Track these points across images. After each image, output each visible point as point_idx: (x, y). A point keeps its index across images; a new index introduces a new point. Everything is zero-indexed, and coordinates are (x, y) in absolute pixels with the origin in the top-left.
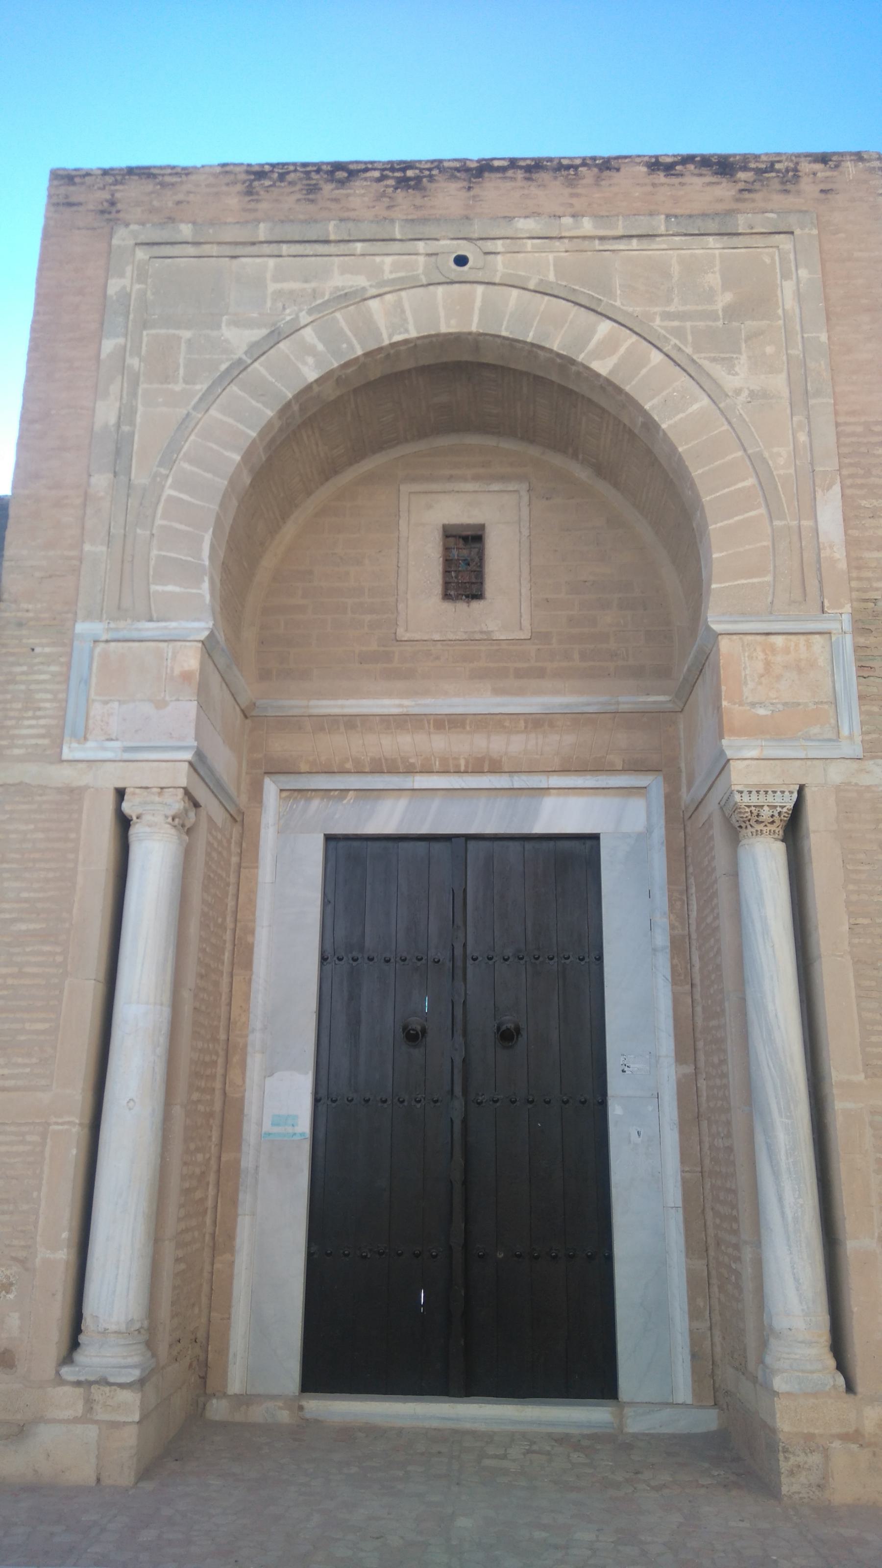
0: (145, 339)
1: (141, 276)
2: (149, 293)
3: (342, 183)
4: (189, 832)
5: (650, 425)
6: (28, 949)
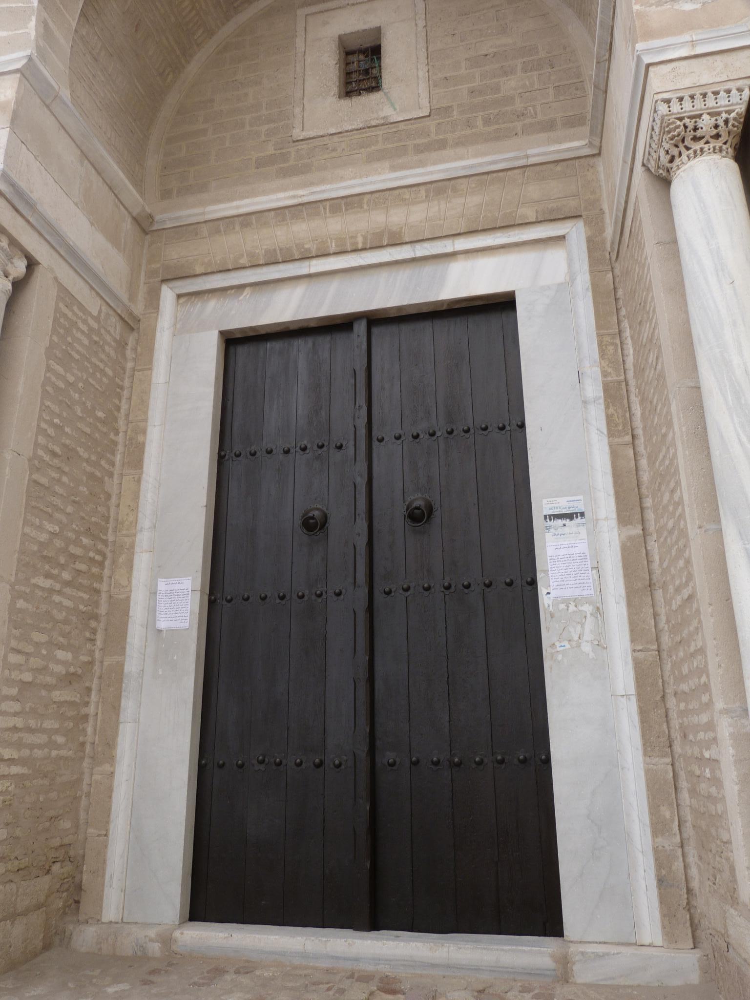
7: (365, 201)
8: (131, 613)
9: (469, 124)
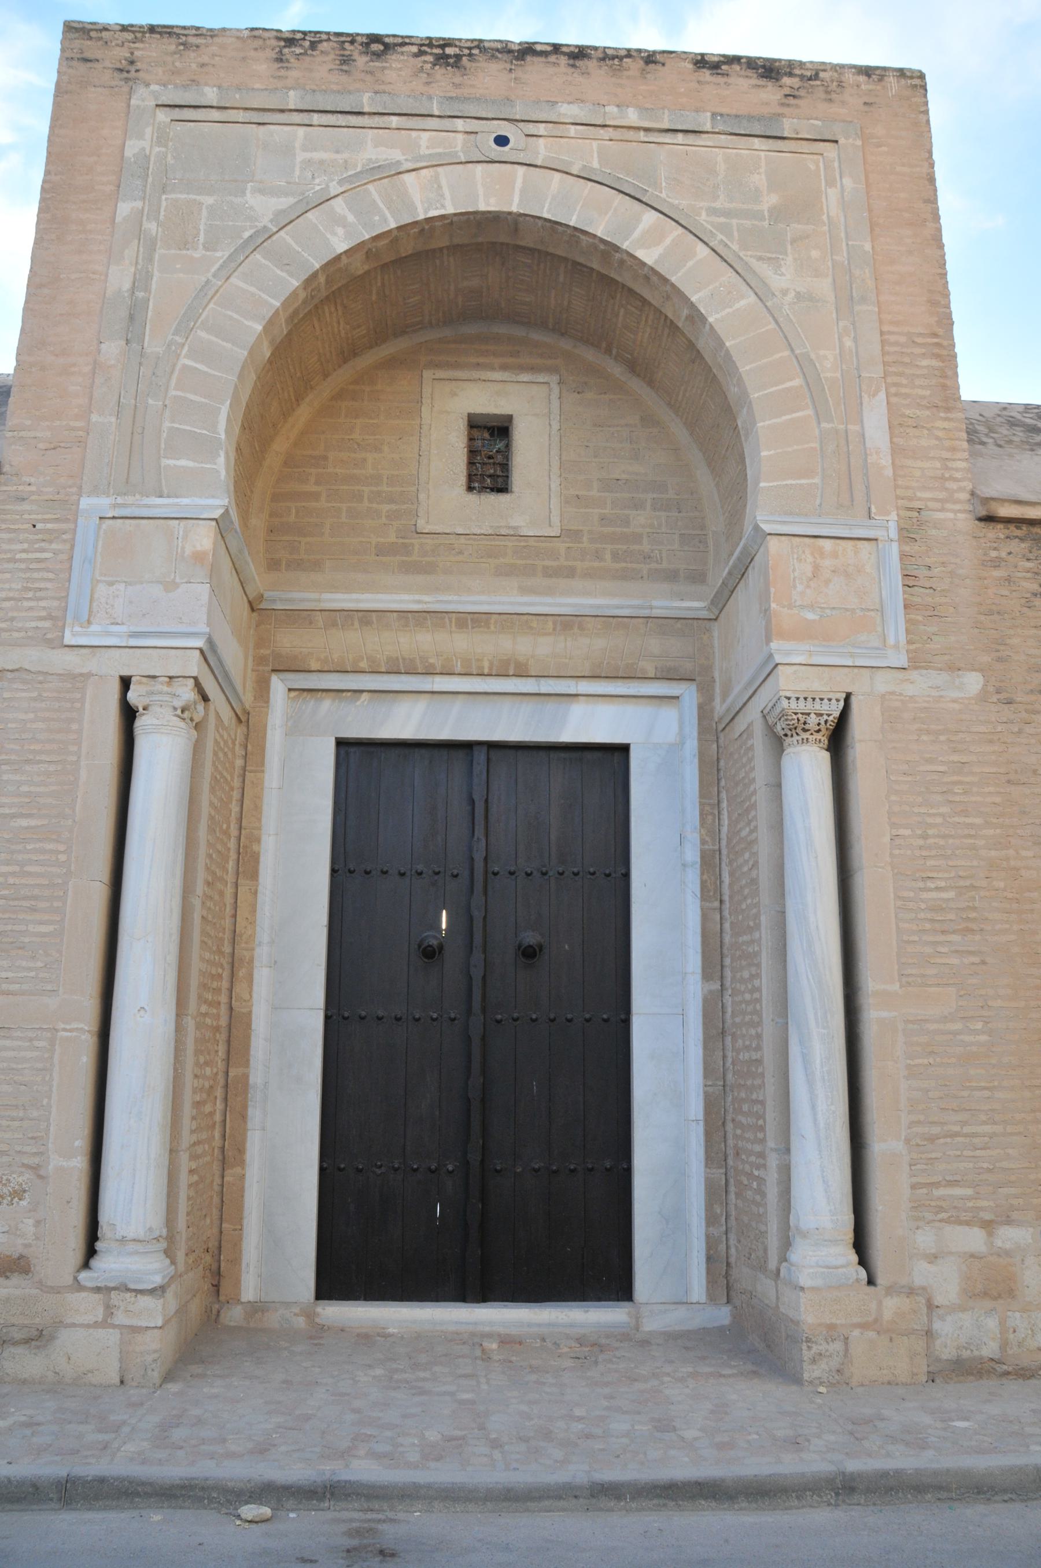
0: (164, 204)
1: (161, 139)
2: (169, 156)
3: (378, 55)
4: (197, 727)
5: (696, 317)
6: (29, 847)
7: (492, 621)
8: (253, 1026)
9: (598, 556)
